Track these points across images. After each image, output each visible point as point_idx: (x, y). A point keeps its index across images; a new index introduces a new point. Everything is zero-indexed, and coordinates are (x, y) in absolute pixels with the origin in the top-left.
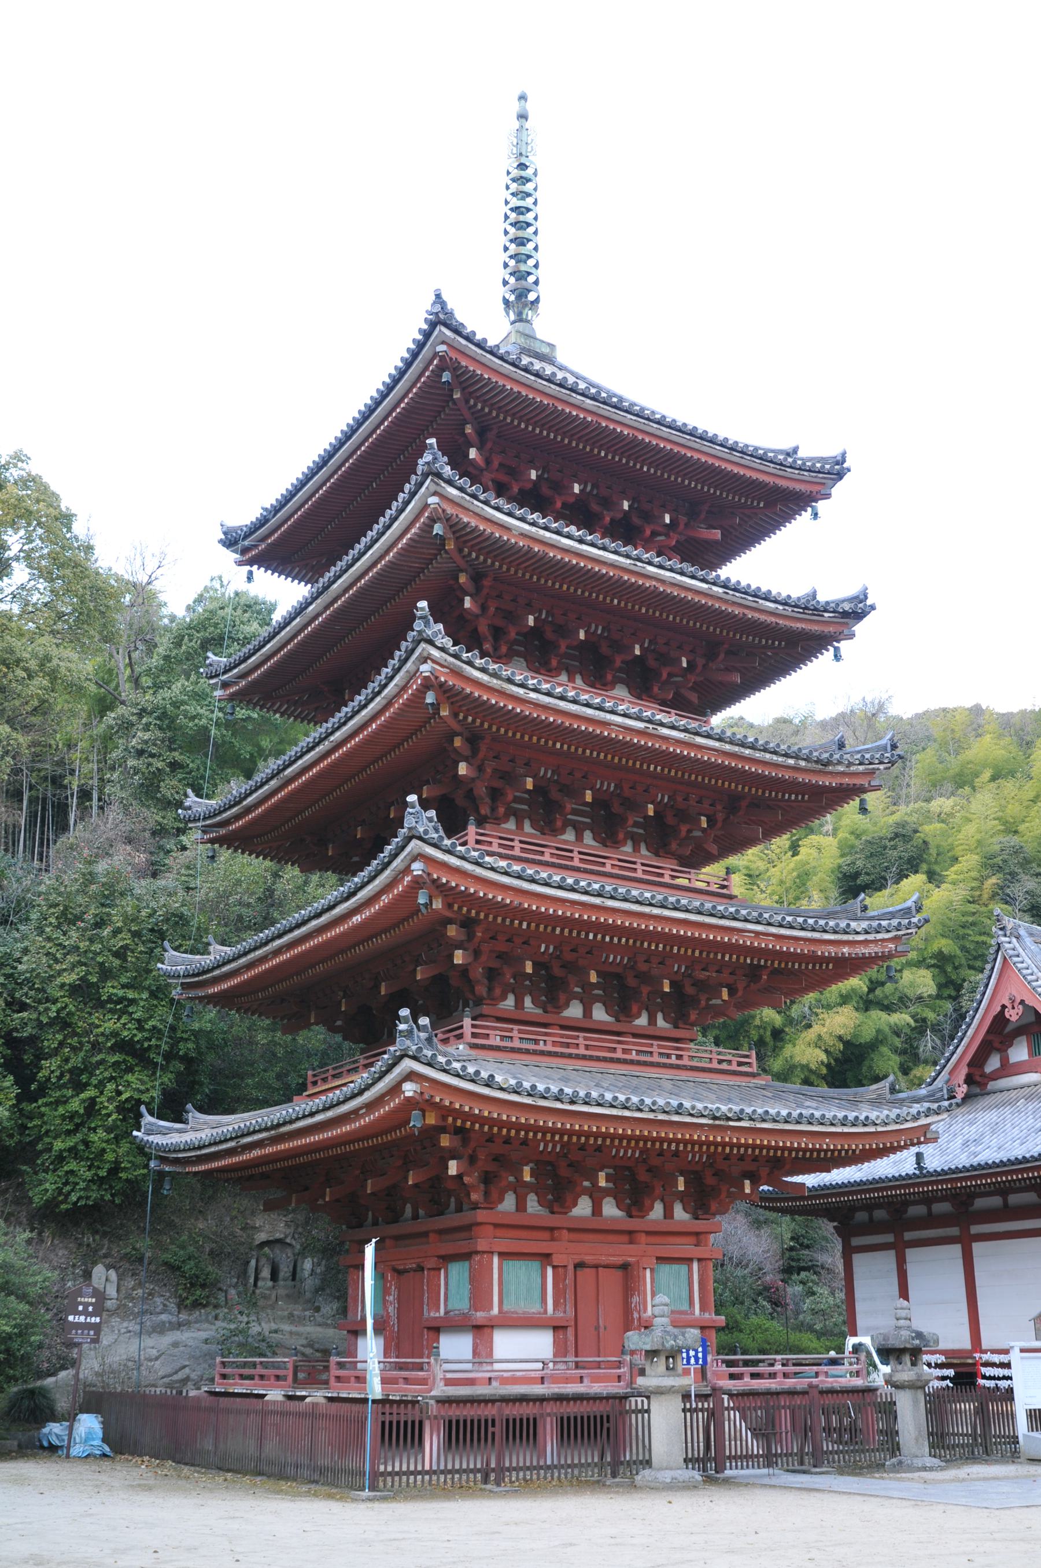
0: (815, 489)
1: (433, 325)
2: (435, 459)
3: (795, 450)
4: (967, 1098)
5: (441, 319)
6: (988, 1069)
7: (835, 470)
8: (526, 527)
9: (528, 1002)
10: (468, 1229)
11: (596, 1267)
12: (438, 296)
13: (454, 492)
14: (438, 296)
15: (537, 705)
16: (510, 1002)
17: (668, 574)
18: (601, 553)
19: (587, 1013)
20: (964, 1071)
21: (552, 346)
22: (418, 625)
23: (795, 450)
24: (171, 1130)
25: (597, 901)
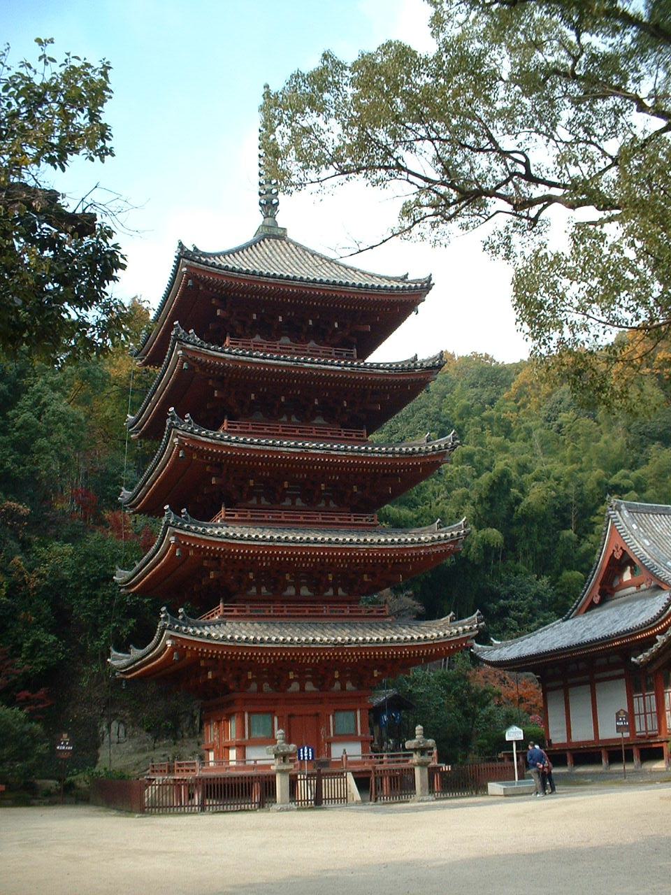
0: (414, 298)
1: (179, 258)
2: (178, 331)
3: (406, 276)
4: (603, 601)
5: (185, 255)
6: (614, 586)
7: (425, 287)
8: (232, 356)
9: (264, 590)
10: (231, 703)
11: (301, 716)
12: (180, 243)
13: (190, 346)
14: (180, 243)
15: (239, 449)
16: (254, 590)
17: (317, 366)
18: (276, 362)
19: (298, 592)
20: (598, 587)
21: (285, 230)
22: (168, 421)
23: (406, 276)
24: (123, 658)
25: (271, 544)
